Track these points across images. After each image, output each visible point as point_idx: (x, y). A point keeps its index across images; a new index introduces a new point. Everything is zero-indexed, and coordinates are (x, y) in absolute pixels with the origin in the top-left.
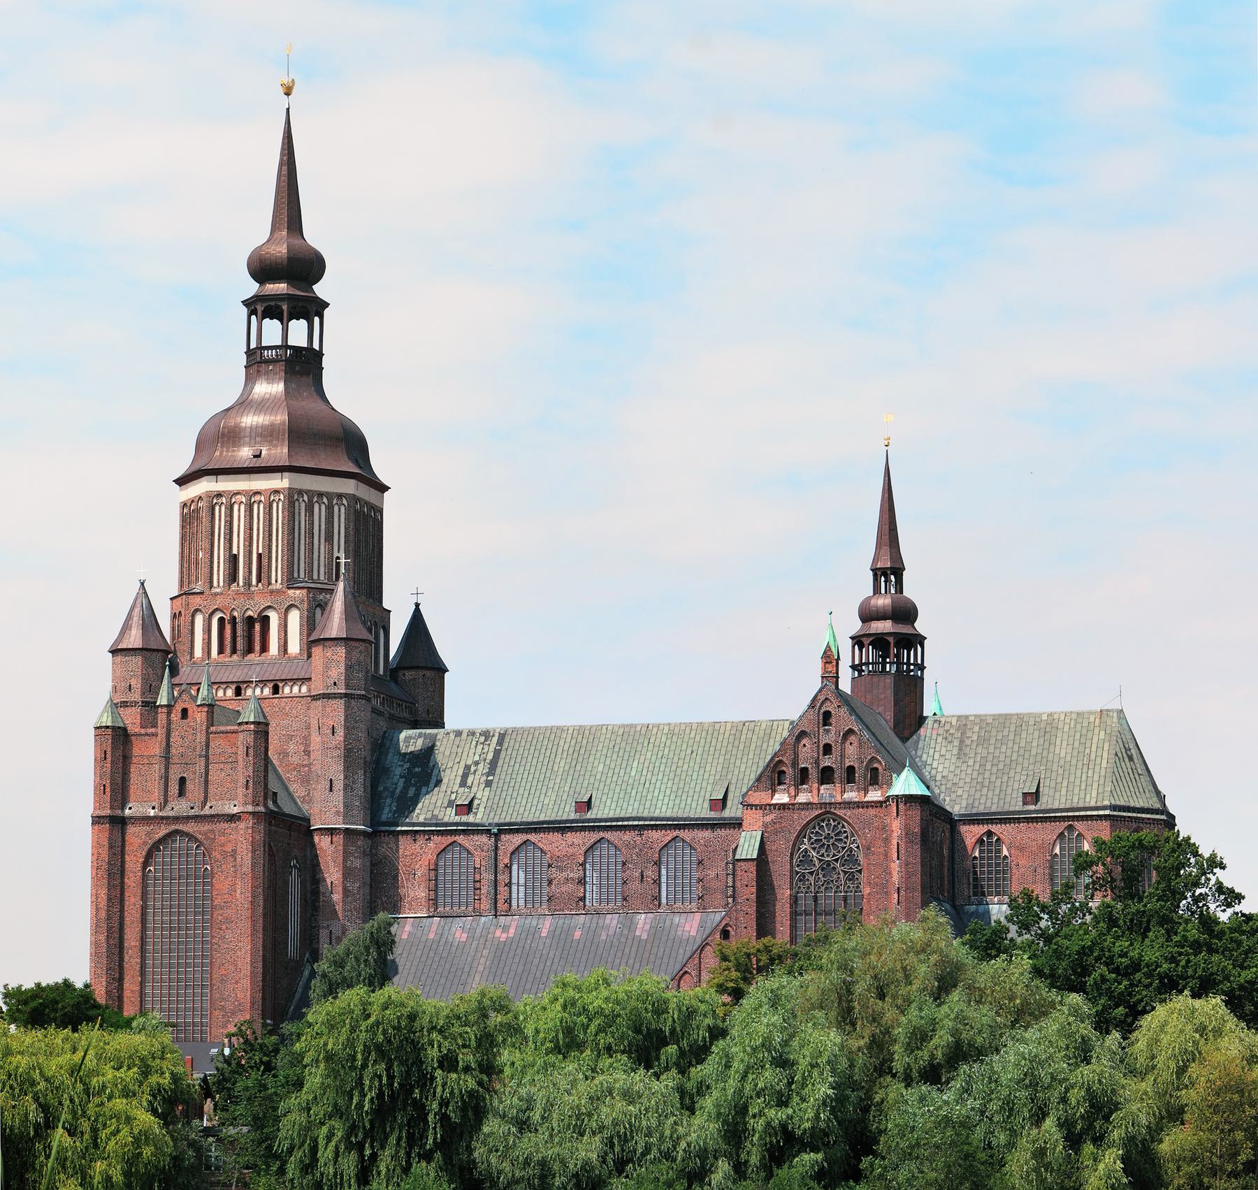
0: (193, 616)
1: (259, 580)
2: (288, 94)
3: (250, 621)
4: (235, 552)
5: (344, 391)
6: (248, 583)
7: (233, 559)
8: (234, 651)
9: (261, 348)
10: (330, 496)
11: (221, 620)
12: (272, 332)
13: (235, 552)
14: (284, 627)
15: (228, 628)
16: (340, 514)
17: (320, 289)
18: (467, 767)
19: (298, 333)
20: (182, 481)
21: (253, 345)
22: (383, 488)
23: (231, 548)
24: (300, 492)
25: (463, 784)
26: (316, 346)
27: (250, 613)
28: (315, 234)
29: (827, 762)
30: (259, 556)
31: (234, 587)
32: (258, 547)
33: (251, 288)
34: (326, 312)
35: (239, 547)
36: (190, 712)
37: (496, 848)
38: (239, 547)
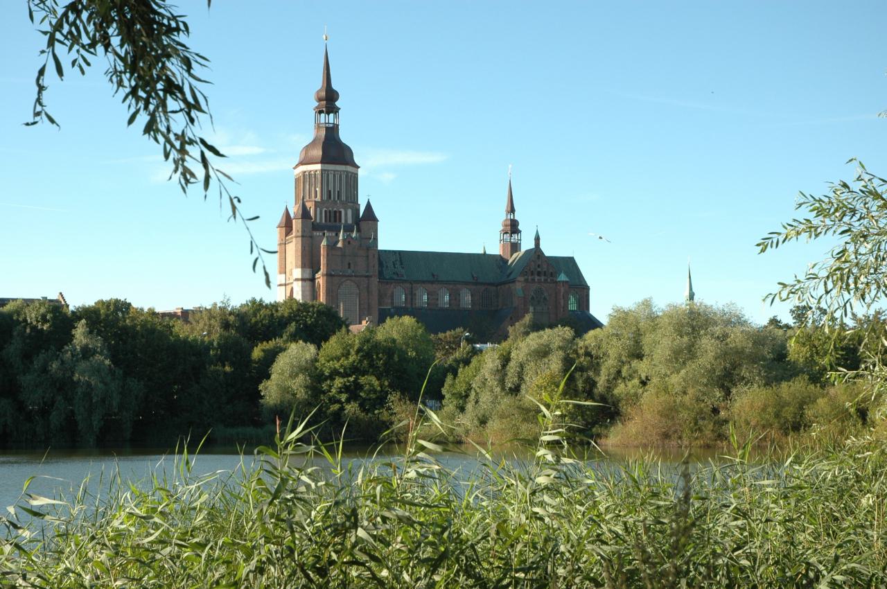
3: (335, 212)
5: (344, 137)
7: (330, 192)
8: (330, 221)
11: (326, 211)
14: (346, 214)
15: (328, 214)
17: (338, 104)
18: (393, 262)
24: (325, 170)
25: (395, 267)
27: (335, 209)
28: (335, 86)
29: (539, 270)
30: (338, 192)
32: (337, 189)
33: (317, 104)
35: (331, 188)
36: (351, 242)
37: (412, 288)
38: (331, 188)
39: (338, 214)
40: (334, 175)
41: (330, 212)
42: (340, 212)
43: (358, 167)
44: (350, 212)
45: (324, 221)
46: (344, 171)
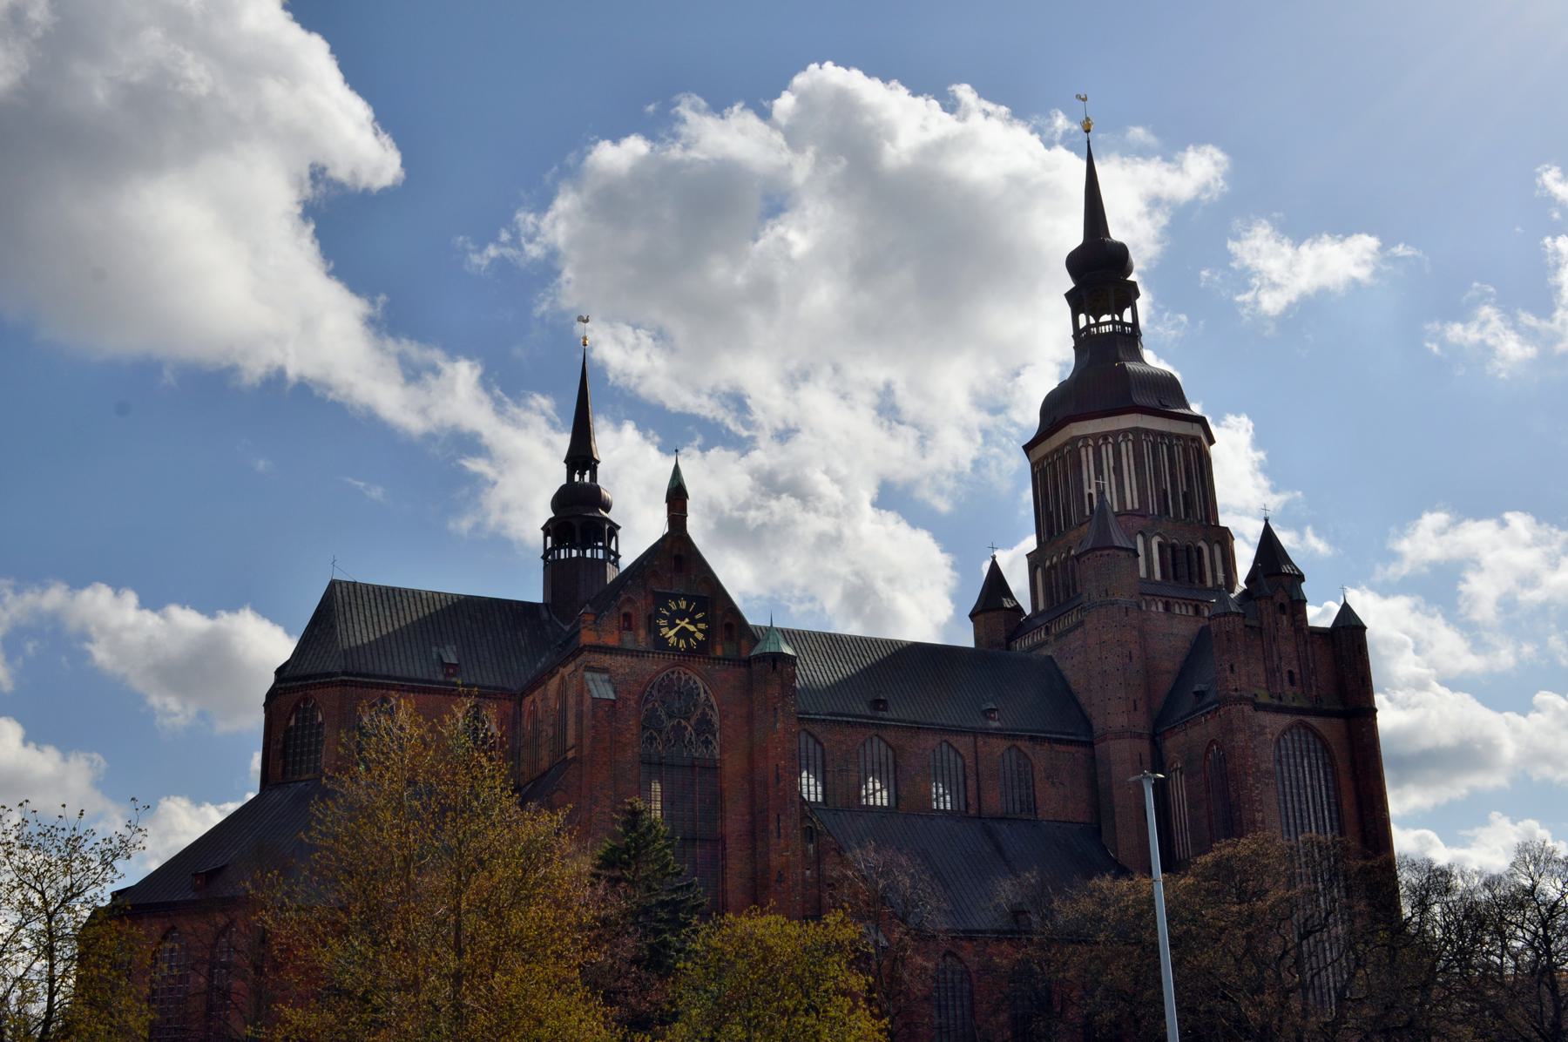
1: (1187, 515)
6: (1177, 515)
7: (1165, 492)
11: (1160, 545)
30: (1185, 495)
32: (1182, 487)
40: (1170, 448)
41: (1173, 546)
42: (1200, 551)
43: (1211, 441)
45: (1158, 576)
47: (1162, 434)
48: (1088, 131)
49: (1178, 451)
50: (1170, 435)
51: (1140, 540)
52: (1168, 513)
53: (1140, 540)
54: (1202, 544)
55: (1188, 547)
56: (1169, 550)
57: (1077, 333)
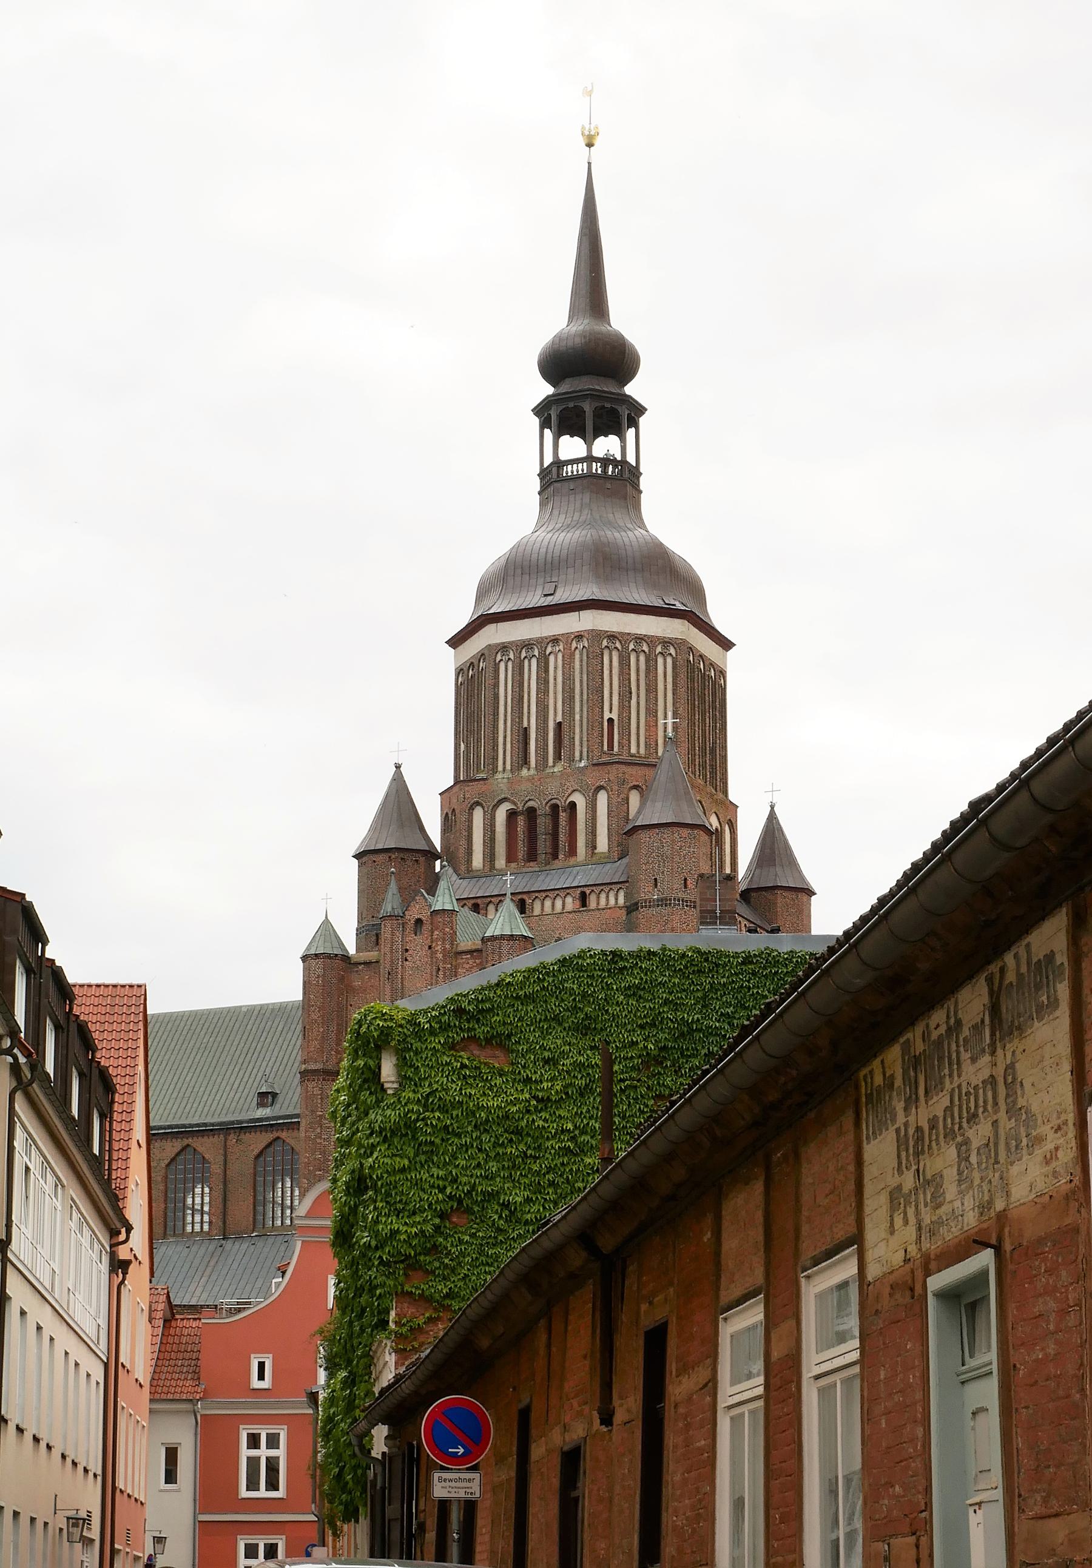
0: (472, 808)
1: (558, 757)
2: (590, 145)
4: (525, 725)
5: (670, 514)
7: (526, 731)
9: (558, 464)
10: (651, 641)
11: (512, 815)
12: (572, 447)
13: (525, 725)
16: (664, 667)
19: (606, 445)
20: (455, 642)
21: (548, 460)
22: (726, 644)
23: (521, 718)
26: (631, 459)
28: (625, 318)
31: (524, 772)
34: (642, 421)
39: (563, 816)
41: (531, 813)
42: (573, 805)
44: (602, 798)
46: (579, 637)
47: (528, 645)
48: (590, 145)
49: (555, 663)
50: (542, 642)
51: (478, 815)
52: (526, 761)
53: (478, 815)
54: (579, 800)
55: (555, 808)
56: (521, 821)
57: (553, 478)
